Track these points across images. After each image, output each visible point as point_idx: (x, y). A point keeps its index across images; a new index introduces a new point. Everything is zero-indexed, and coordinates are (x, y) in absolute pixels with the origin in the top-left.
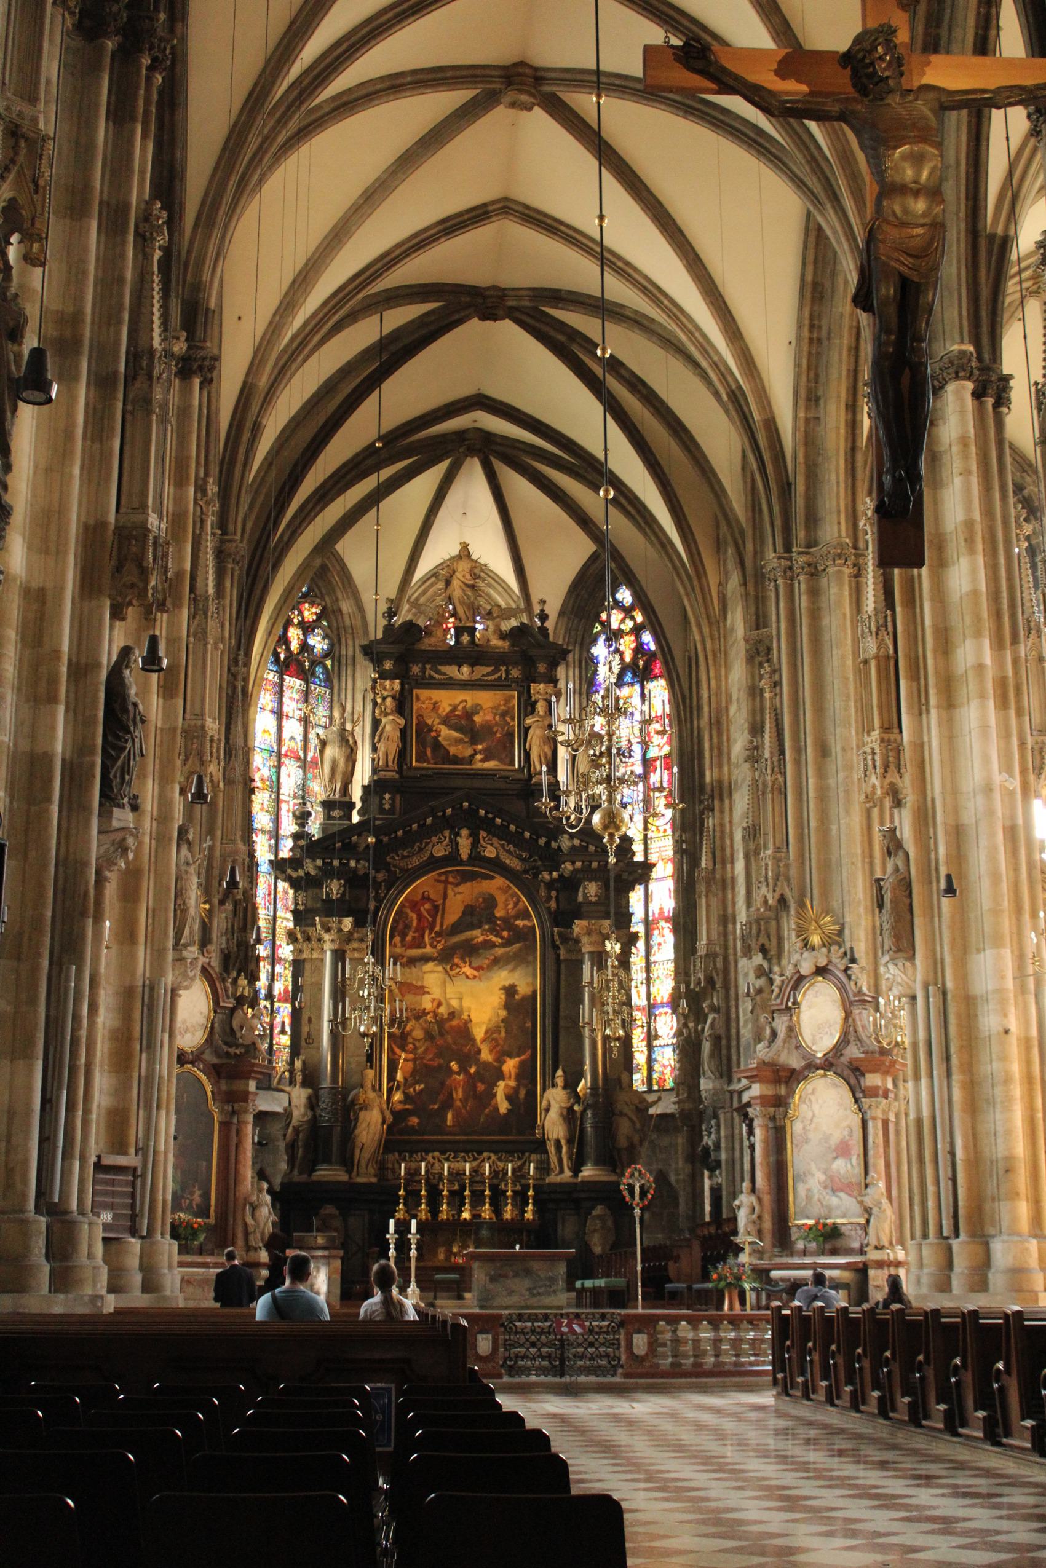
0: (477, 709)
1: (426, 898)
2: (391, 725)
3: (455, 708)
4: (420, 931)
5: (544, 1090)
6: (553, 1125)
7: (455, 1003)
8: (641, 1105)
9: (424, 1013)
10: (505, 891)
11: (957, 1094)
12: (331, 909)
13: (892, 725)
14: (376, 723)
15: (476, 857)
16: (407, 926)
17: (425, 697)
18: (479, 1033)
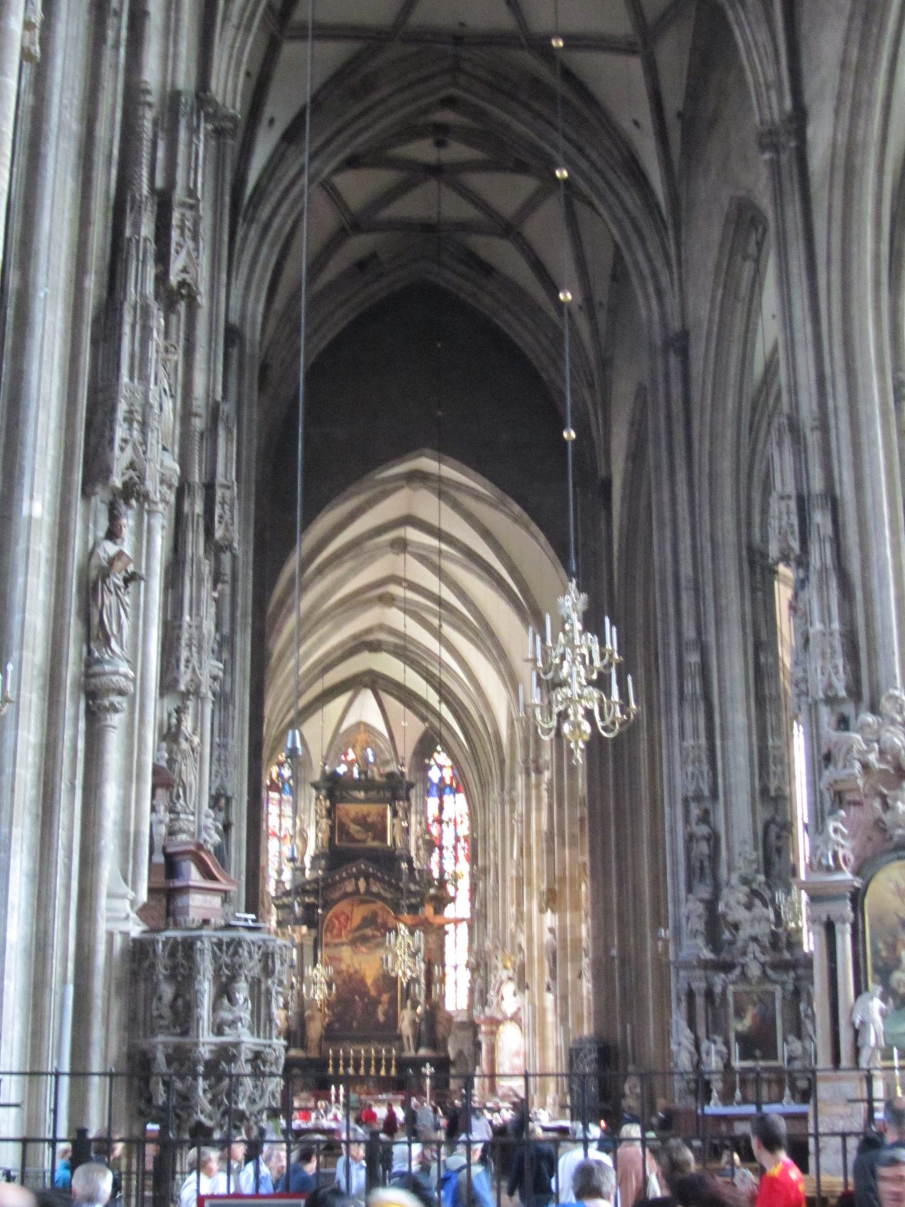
0: (368, 814)
1: (343, 913)
2: (324, 823)
3: (357, 813)
4: (340, 931)
5: (402, 1008)
6: (405, 1026)
7: (357, 966)
8: (449, 1018)
9: (342, 971)
10: (382, 908)
11: (537, 1044)
12: (297, 922)
13: (519, 904)
14: (317, 823)
15: (368, 891)
16: (333, 927)
17: (343, 807)
18: (369, 981)
